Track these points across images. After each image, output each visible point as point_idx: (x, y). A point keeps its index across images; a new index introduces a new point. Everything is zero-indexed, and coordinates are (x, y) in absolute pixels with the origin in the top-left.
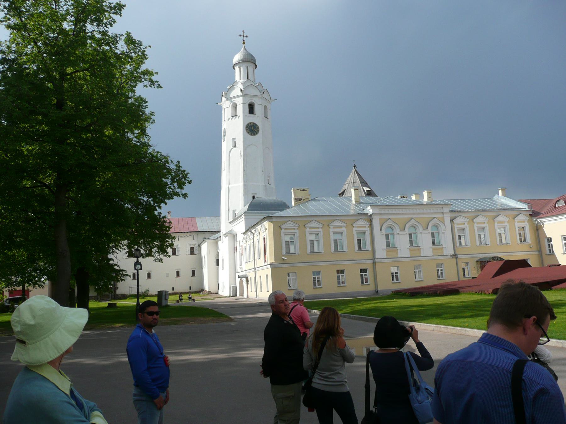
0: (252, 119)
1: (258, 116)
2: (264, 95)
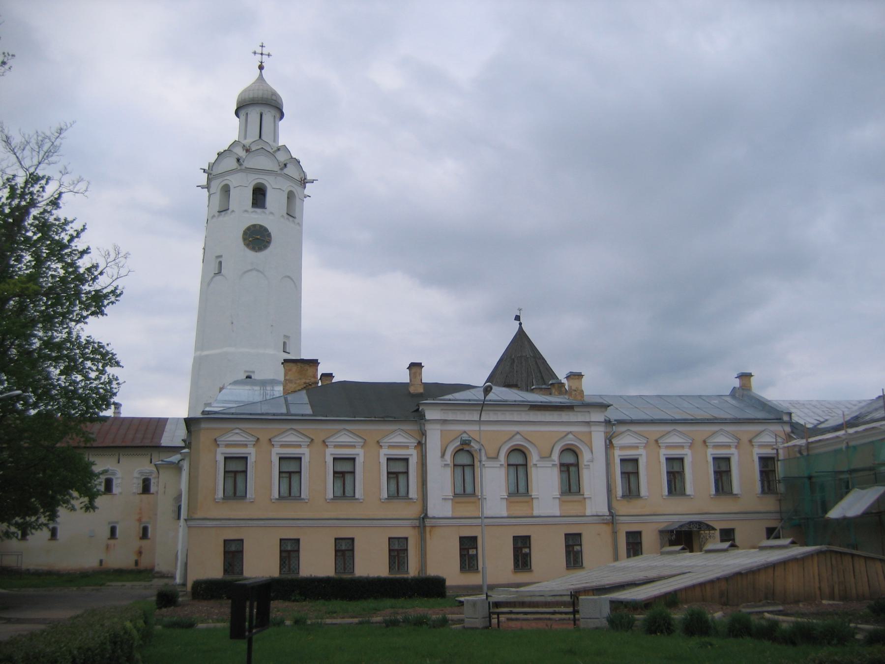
0: (258, 218)
1: (272, 213)
2: (286, 171)
